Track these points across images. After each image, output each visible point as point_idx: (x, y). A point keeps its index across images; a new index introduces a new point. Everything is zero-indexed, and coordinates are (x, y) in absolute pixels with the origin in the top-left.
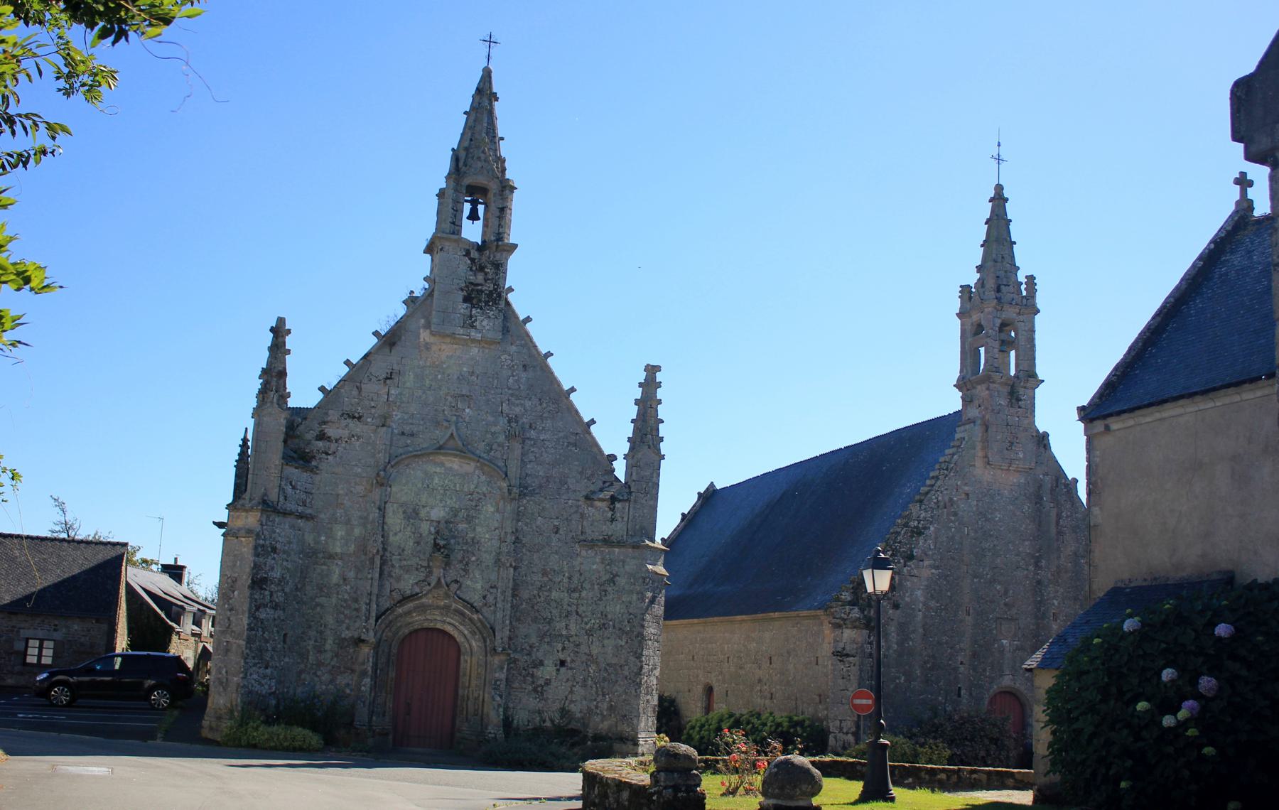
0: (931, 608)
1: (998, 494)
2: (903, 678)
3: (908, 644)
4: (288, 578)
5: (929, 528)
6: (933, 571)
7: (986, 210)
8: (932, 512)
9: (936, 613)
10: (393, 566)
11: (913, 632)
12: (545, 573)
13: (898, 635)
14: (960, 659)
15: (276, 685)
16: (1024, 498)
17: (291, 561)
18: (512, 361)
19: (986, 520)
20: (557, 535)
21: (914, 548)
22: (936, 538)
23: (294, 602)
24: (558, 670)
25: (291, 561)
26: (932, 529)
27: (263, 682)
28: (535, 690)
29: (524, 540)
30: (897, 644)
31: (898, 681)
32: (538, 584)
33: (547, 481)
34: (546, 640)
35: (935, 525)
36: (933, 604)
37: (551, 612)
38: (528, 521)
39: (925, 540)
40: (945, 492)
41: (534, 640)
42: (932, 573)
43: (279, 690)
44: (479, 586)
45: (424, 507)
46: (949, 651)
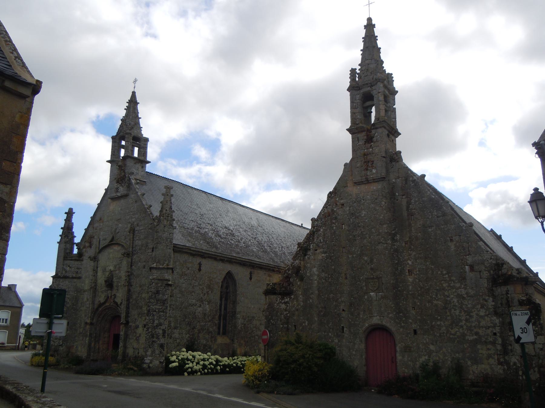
0: (323, 278)
1: (363, 200)
2: (307, 322)
3: (309, 301)
4: (68, 301)
5: (320, 230)
6: (323, 255)
7: (363, 33)
8: (321, 220)
9: (326, 280)
10: (99, 292)
11: (312, 294)
12: (140, 286)
13: (303, 296)
14: (342, 307)
15: (62, 342)
16: (382, 197)
17: (70, 295)
18: (132, 201)
19: (355, 218)
20: (145, 269)
21: (311, 243)
22: (324, 235)
23: (72, 310)
24: (143, 329)
25: (70, 295)
26: (322, 230)
27: (55, 341)
28: (136, 339)
29: (135, 273)
30: (303, 302)
31: (304, 324)
32: (138, 291)
33: (142, 247)
34: (140, 316)
35: (324, 228)
36: (323, 275)
37: (142, 303)
38: (136, 265)
39: (318, 238)
40: (329, 207)
41: (136, 317)
42: (322, 257)
43: (64, 344)
44: (121, 295)
45: (107, 266)
46: (334, 303)
